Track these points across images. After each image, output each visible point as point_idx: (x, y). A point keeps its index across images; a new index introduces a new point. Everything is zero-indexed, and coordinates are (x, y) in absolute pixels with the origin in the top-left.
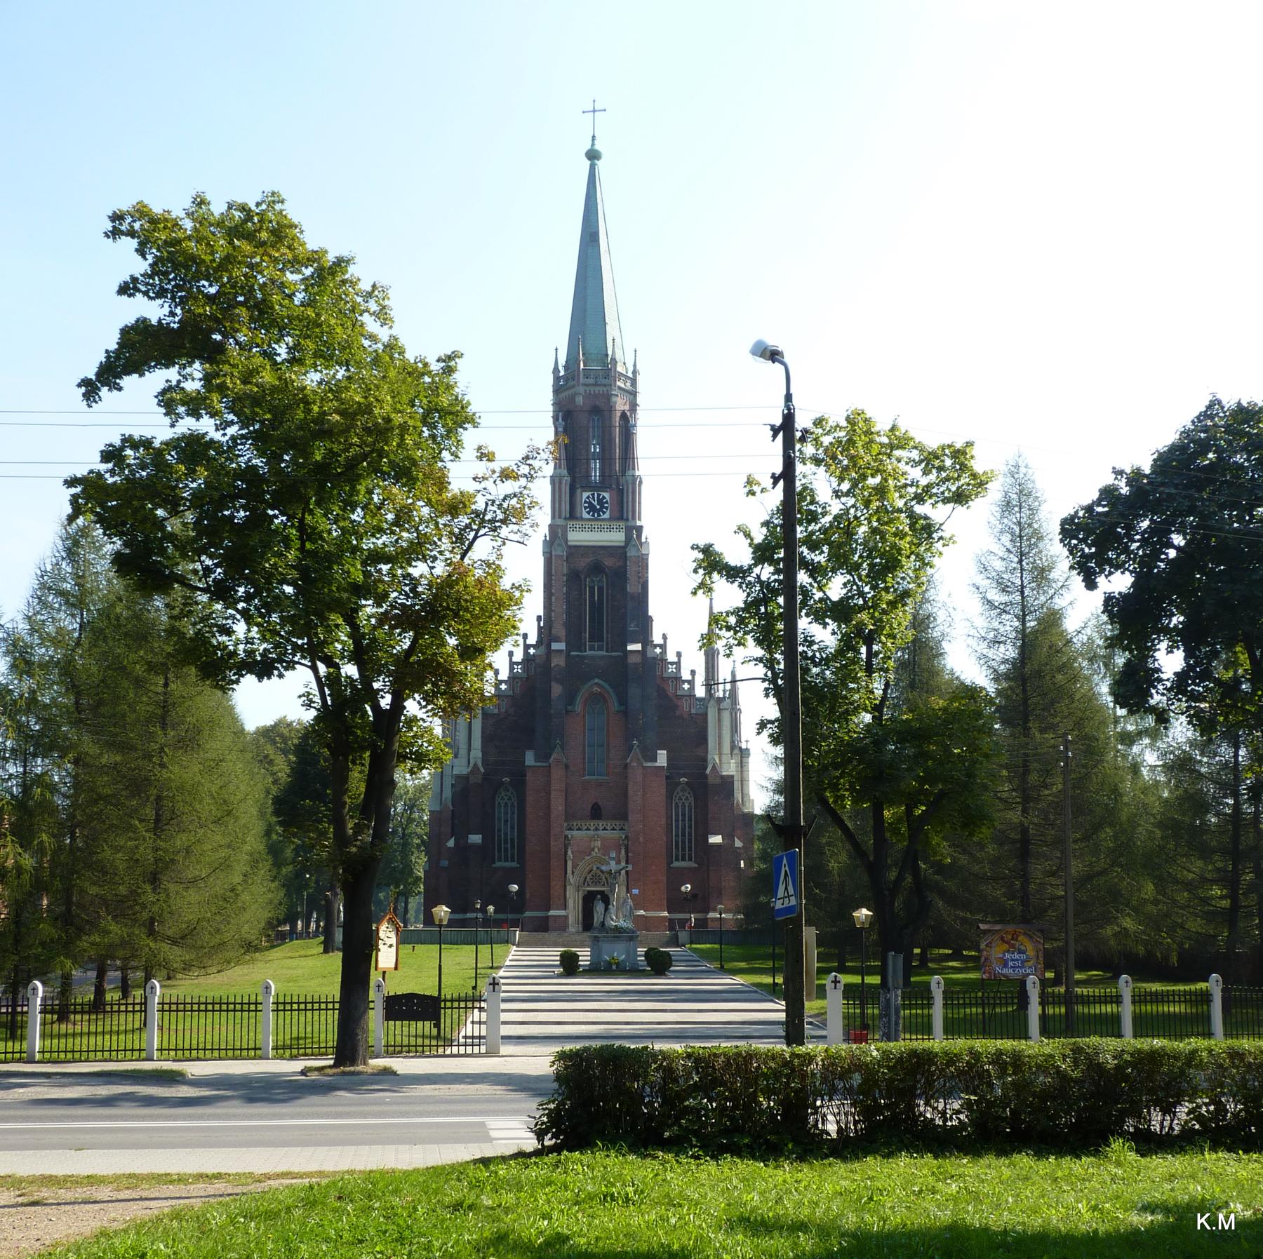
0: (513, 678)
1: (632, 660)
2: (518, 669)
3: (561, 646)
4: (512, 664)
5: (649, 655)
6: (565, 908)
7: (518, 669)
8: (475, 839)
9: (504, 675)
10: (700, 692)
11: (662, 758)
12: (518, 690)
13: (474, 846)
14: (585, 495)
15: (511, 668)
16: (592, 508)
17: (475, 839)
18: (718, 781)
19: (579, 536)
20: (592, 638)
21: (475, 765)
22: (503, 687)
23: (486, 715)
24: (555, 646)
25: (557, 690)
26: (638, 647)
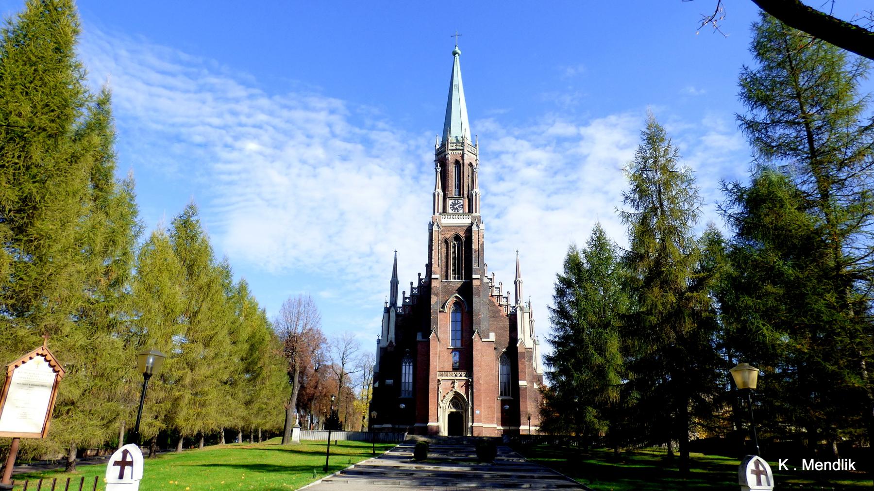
0: (412, 295)
1: (475, 283)
2: (415, 291)
3: (437, 276)
4: (412, 289)
5: (485, 280)
6: (438, 420)
7: (415, 291)
8: (389, 382)
9: (408, 295)
10: (512, 302)
11: (492, 337)
12: (415, 302)
13: (388, 386)
14: (451, 202)
15: (412, 291)
16: (453, 208)
17: (389, 382)
18: (523, 351)
19: (446, 221)
20: (454, 273)
21: (391, 342)
22: (407, 300)
23: (398, 315)
24: (433, 276)
25: (434, 299)
26: (478, 276)
